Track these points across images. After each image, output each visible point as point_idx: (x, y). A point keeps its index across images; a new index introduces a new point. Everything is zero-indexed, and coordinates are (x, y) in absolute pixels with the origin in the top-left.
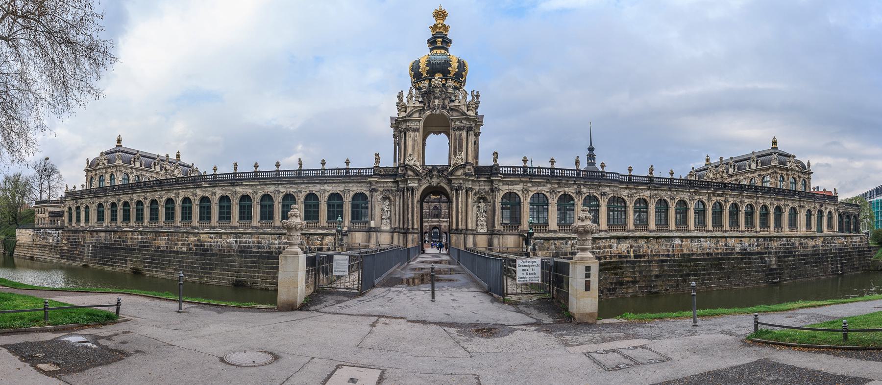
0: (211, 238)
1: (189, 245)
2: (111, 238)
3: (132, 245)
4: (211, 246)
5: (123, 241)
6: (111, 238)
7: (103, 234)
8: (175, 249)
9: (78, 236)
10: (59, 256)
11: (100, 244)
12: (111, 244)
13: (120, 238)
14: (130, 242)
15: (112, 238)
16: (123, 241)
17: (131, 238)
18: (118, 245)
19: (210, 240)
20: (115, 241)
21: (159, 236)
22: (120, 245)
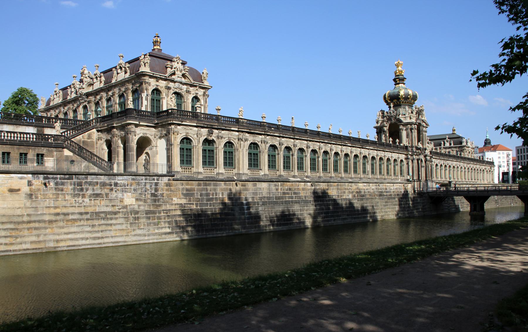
0: (364, 186)
1: (352, 192)
2: (277, 189)
3: (305, 197)
4: (365, 192)
5: (295, 193)
6: (277, 189)
7: (264, 185)
8: (344, 197)
9: (215, 190)
10: (168, 230)
11: (261, 198)
12: (279, 198)
13: (290, 189)
14: (302, 194)
15: (279, 191)
16: (295, 193)
17: (303, 189)
18: (289, 198)
19: (364, 187)
20: (284, 193)
21: (331, 186)
22: (292, 198)
